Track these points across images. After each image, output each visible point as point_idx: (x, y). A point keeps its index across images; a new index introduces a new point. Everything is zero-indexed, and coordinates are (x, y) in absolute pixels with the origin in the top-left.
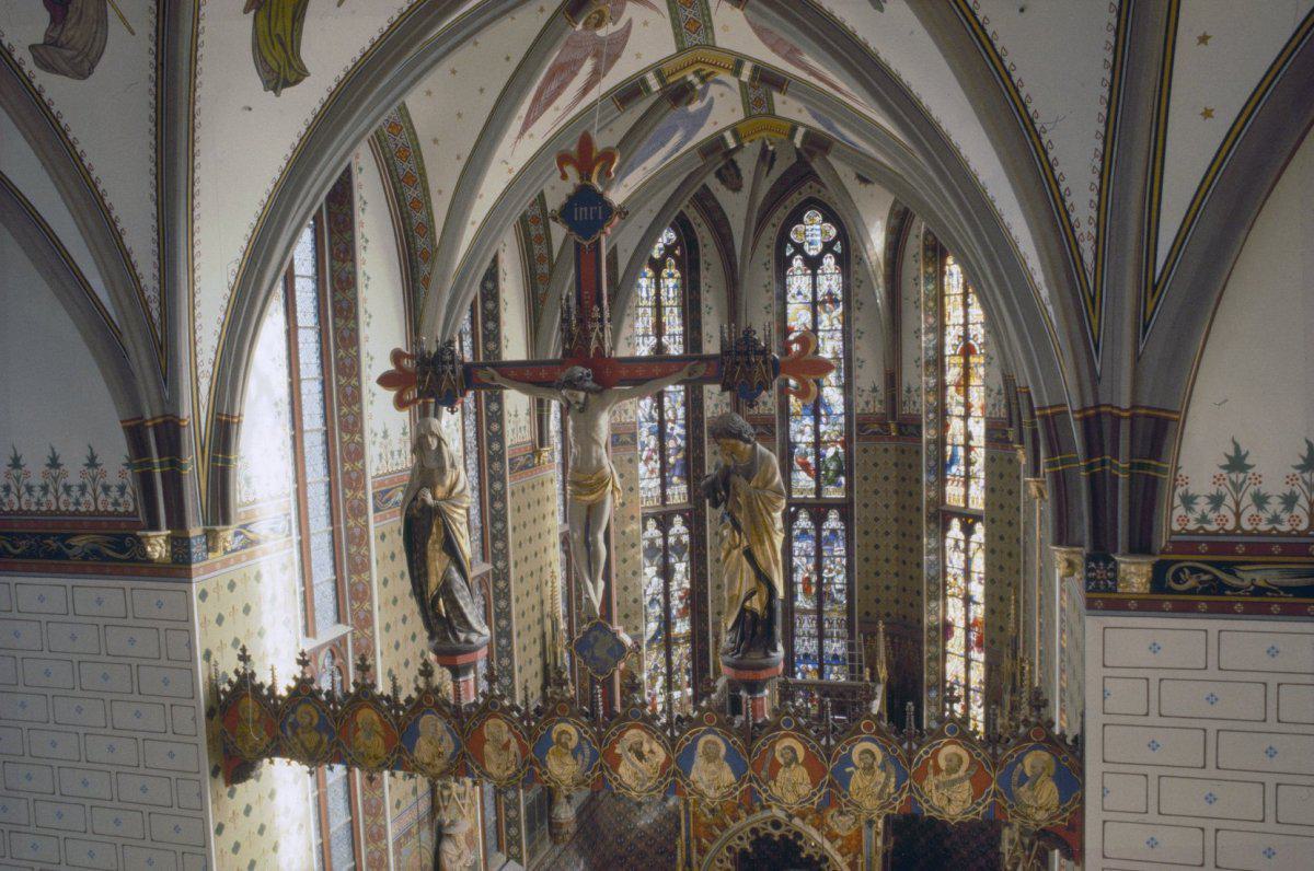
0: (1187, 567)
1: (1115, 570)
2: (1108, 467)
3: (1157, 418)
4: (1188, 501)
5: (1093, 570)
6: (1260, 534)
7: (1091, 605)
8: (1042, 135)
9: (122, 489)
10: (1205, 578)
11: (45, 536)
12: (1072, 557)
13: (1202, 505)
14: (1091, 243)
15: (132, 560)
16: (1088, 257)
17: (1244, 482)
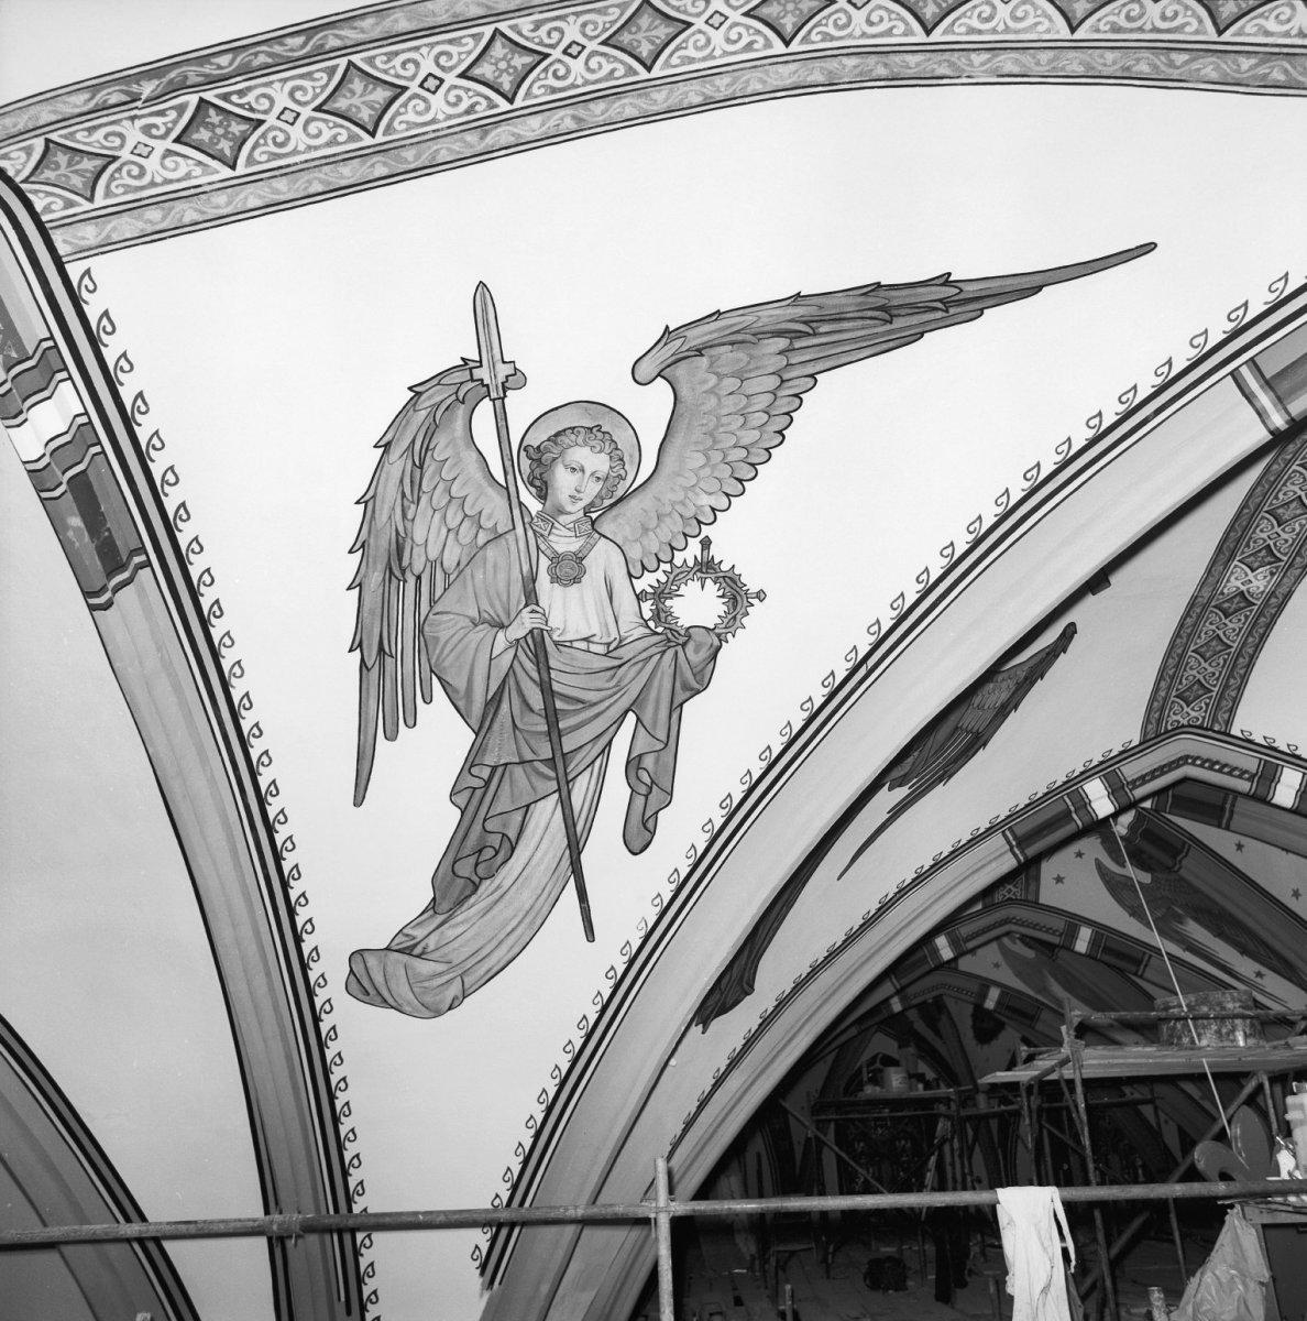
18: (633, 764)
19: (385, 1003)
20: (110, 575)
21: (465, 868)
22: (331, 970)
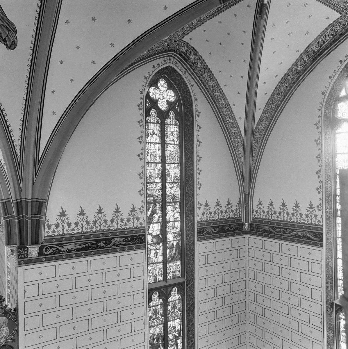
0: (49, 247)
1: (27, 251)
2: (24, 218)
3: (40, 202)
4: (49, 226)
5: (20, 251)
6: (69, 234)
7: (19, 264)
8: (3, 111)
10: (54, 249)
12: (12, 248)
13: (53, 228)
14: (19, 147)
16: (18, 152)
17: (119, 215)
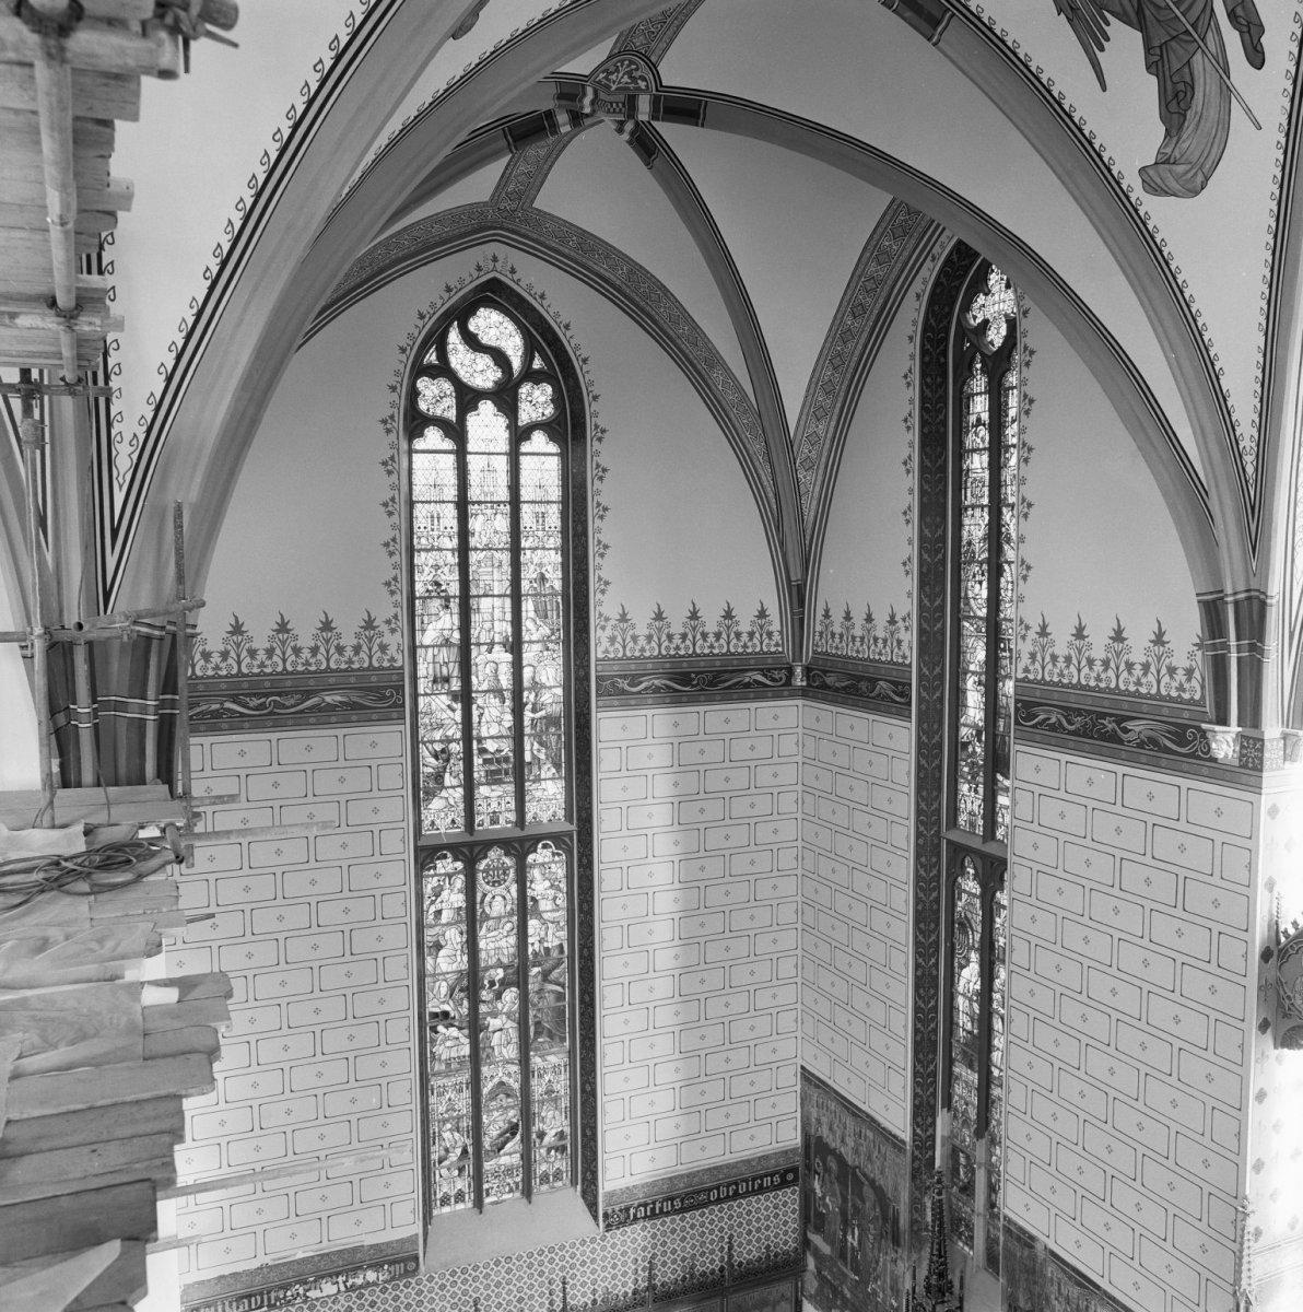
9: (1189, 672)
11: (1104, 715)
15: (1193, 755)
18: (1232, 16)
19: (1167, 194)
20: (935, 29)
21: (1173, 107)
22: (1132, 182)
